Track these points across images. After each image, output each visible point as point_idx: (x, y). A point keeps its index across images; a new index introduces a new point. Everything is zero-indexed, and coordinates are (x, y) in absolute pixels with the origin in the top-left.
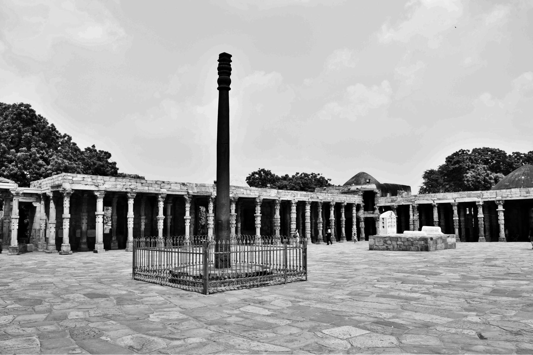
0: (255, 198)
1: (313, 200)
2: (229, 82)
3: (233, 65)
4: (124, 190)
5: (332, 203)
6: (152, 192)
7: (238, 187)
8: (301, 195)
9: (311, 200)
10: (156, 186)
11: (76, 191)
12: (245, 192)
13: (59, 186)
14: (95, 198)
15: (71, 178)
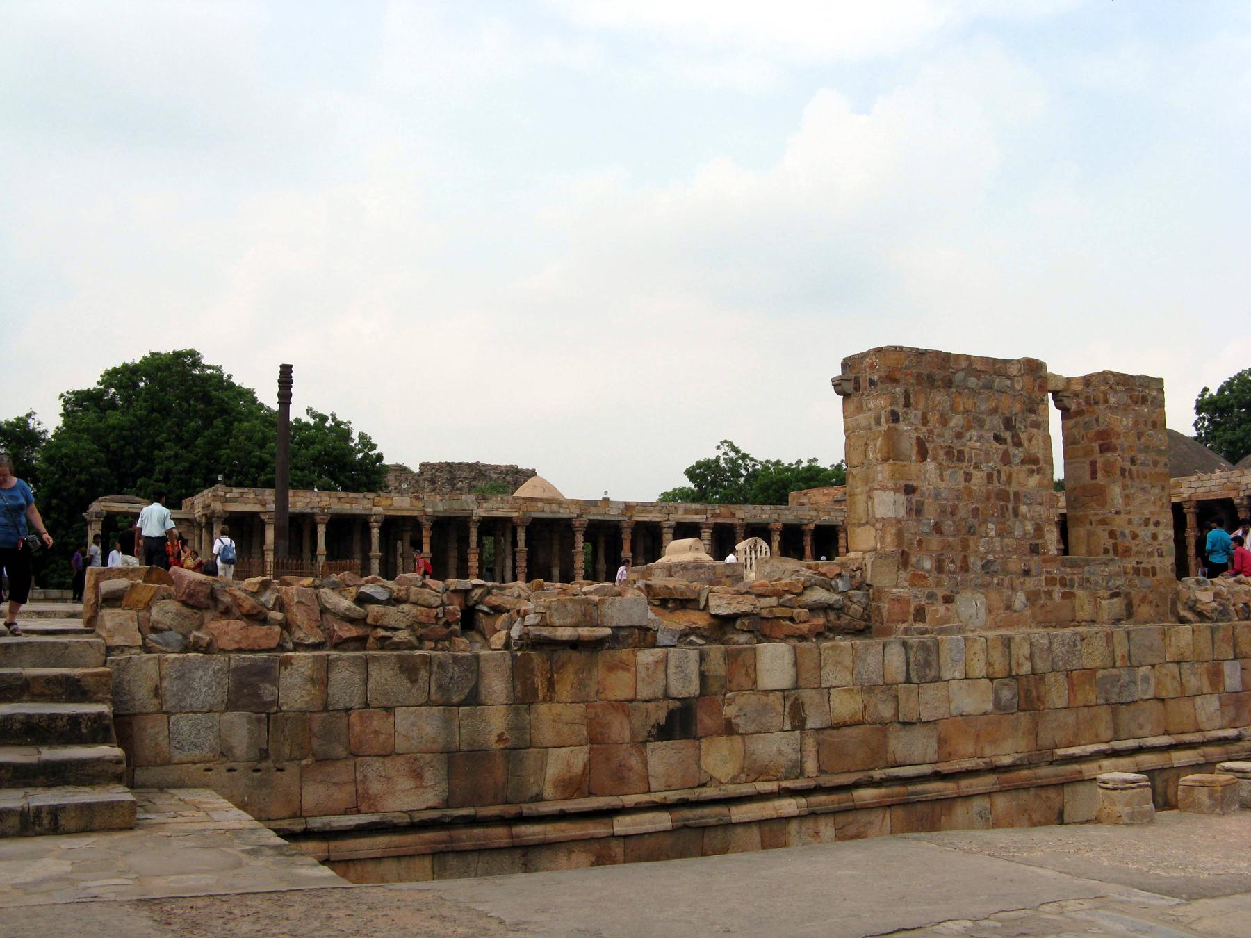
0: (570, 519)
1: (719, 520)
2: (290, 395)
3: (295, 376)
4: (308, 510)
5: (772, 526)
6: (358, 512)
7: (532, 499)
8: (686, 511)
9: (712, 521)
10: (366, 501)
11: (231, 513)
12: (547, 508)
13: (209, 506)
14: (263, 524)
15: (222, 494)
